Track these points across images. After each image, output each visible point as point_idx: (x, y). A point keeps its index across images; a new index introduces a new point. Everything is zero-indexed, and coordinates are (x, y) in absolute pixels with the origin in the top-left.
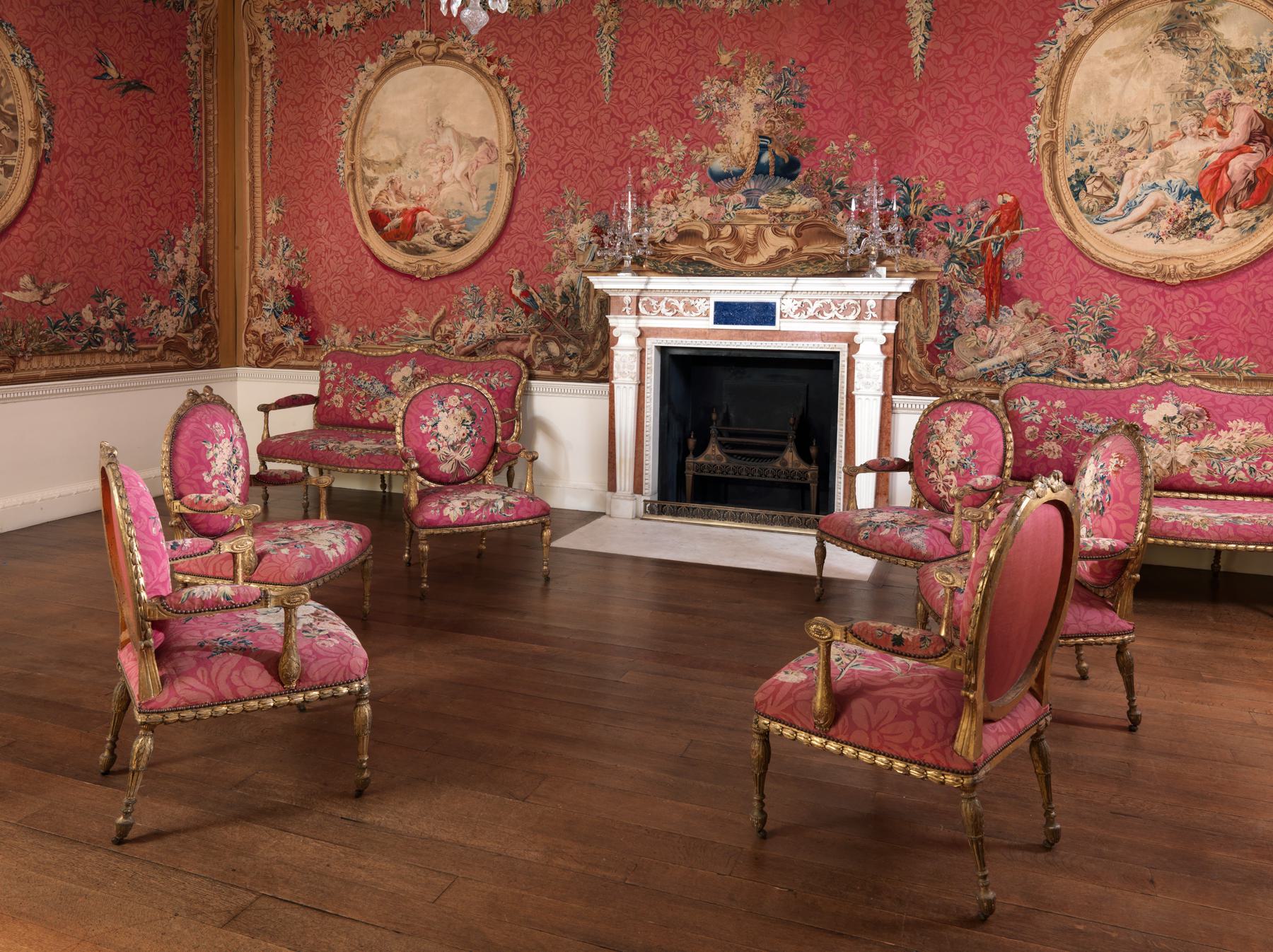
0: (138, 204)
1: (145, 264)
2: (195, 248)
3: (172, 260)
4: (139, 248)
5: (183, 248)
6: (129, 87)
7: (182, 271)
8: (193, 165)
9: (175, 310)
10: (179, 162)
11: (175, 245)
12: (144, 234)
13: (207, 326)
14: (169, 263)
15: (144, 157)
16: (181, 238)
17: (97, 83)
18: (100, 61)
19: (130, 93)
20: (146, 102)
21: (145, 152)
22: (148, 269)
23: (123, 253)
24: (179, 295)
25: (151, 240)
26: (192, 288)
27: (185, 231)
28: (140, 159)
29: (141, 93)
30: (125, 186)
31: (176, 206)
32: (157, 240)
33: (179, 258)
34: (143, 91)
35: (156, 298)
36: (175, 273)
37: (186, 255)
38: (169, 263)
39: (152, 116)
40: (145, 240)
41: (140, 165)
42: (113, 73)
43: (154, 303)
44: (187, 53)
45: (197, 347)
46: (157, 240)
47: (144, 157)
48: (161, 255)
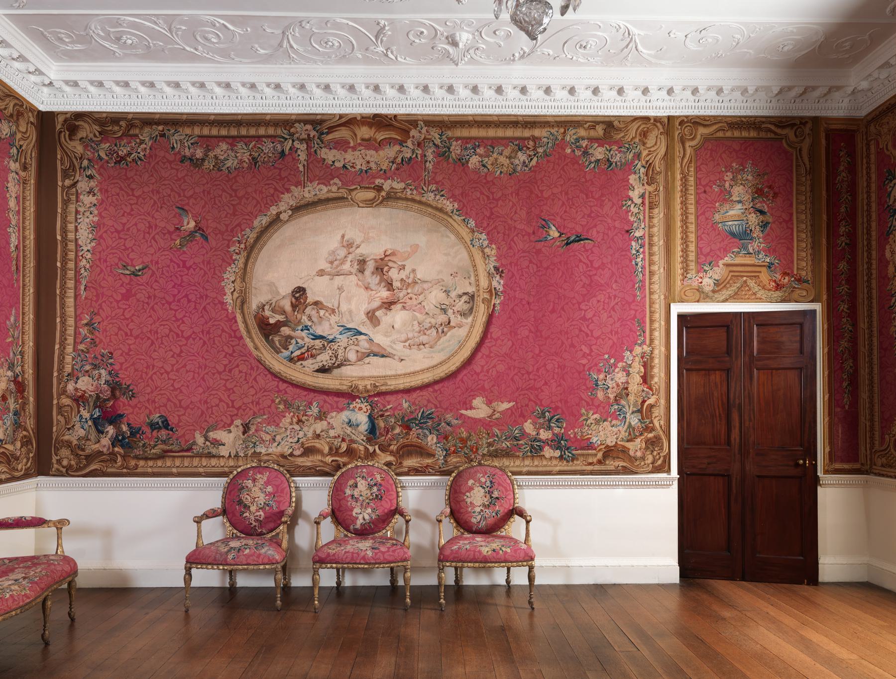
2: (637, 368)
8: (635, 296)
11: (616, 367)
13: (651, 435)
26: (635, 405)
33: (620, 377)
37: (628, 374)
44: (631, 199)
45: (639, 454)
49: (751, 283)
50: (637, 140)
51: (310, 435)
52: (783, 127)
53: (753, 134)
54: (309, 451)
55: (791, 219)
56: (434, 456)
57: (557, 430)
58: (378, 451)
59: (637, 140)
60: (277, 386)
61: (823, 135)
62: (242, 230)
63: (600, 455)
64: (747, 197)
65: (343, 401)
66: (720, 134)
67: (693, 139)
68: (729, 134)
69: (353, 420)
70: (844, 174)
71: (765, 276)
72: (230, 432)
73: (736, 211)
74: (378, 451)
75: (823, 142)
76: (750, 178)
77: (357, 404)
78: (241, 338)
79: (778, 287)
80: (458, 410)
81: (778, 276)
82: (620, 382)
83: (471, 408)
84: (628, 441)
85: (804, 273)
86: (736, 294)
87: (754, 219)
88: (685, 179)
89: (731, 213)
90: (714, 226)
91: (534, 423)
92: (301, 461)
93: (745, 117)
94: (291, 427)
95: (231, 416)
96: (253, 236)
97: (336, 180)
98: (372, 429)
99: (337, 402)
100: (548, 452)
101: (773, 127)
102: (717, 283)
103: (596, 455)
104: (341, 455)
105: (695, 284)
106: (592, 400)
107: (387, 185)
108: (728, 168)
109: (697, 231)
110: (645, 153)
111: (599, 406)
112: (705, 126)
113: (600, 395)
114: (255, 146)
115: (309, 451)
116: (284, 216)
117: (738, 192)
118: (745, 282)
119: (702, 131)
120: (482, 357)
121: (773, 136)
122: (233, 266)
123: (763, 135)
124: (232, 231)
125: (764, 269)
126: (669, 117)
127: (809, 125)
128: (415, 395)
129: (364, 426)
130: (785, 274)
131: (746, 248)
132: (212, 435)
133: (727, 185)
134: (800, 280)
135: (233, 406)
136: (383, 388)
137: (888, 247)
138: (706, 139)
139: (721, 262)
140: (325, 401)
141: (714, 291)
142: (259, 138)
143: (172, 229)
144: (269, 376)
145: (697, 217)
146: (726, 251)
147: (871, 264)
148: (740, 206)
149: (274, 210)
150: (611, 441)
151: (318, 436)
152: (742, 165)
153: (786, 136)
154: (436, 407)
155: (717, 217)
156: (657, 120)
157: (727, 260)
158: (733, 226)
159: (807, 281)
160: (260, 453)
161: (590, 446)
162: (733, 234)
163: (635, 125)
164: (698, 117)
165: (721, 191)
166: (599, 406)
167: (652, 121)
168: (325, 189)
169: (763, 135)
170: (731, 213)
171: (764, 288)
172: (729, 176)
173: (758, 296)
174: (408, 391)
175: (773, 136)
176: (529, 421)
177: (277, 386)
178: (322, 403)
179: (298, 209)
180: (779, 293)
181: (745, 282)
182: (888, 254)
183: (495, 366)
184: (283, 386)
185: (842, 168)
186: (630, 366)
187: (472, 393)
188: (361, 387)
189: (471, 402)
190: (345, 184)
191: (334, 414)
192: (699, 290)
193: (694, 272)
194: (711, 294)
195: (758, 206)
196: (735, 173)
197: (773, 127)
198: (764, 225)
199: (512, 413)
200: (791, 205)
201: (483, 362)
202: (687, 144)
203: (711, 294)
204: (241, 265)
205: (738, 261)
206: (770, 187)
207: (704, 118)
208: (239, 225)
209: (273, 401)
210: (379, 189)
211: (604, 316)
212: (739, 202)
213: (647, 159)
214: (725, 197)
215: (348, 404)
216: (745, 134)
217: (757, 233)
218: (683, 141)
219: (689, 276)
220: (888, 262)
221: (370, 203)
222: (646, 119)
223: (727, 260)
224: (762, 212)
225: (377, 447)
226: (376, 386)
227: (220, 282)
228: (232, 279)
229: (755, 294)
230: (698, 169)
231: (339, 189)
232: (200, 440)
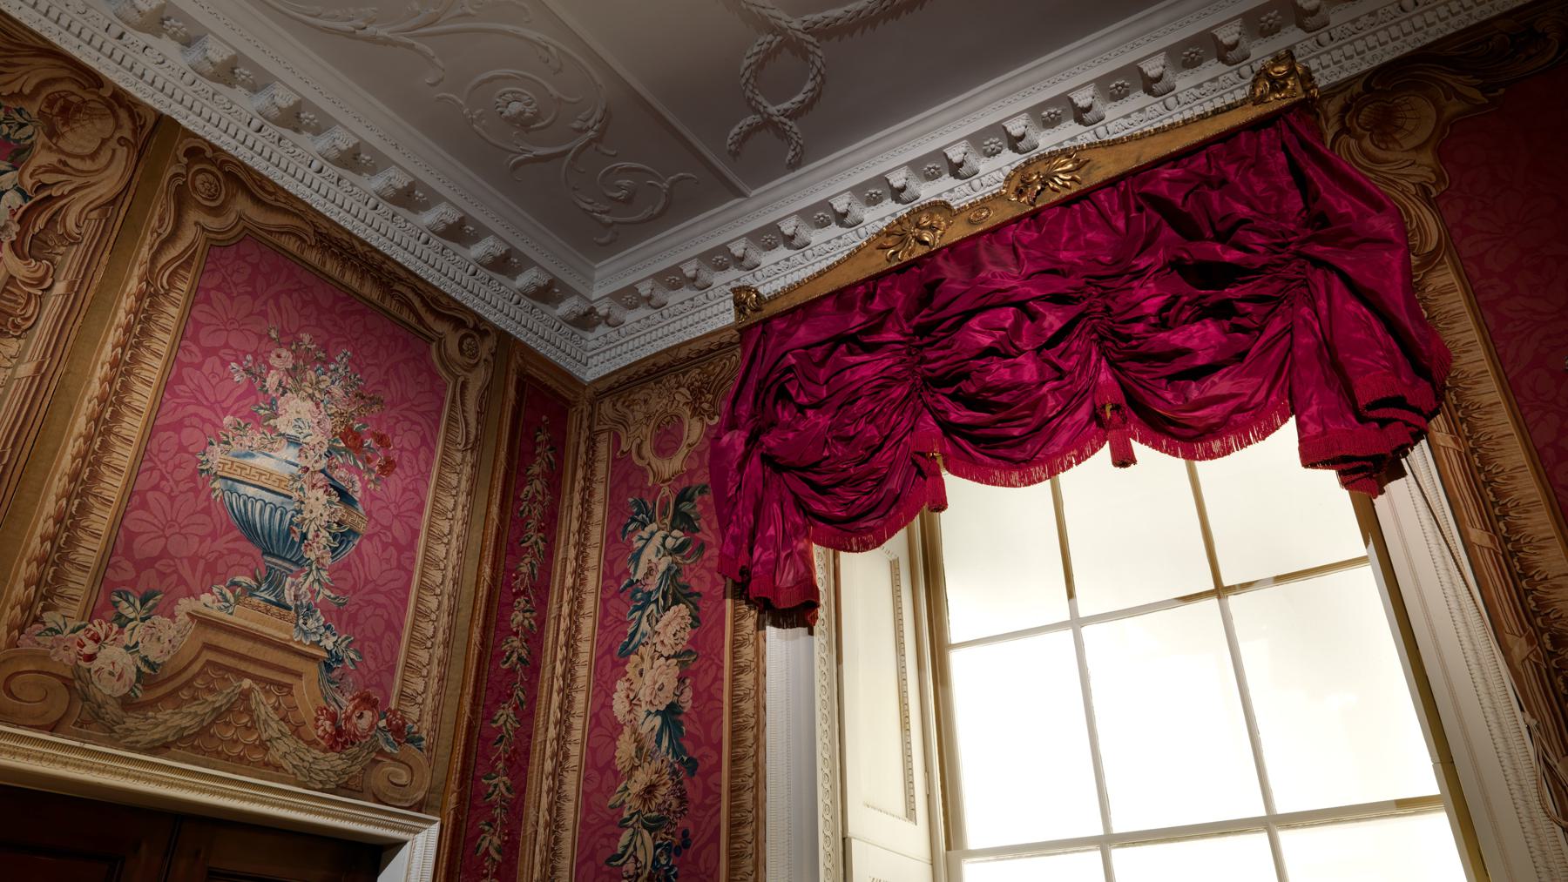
49: (264, 704)
50: (33, 109)
52: (440, 316)
53: (370, 291)
55: (411, 546)
59: (33, 109)
61: (513, 378)
64: (317, 438)
66: (291, 245)
67: (215, 212)
68: (313, 257)
70: (538, 485)
71: (308, 693)
73: (277, 462)
75: (512, 392)
76: (337, 391)
79: (340, 738)
81: (347, 704)
85: (413, 712)
86: (204, 731)
87: (318, 506)
88: (149, 302)
89: (261, 461)
90: (199, 477)
93: (363, 243)
101: (417, 303)
102: (150, 675)
105: (65, 658)
108: (288, 338)
109: (137, 471)
110: (43, 158)
112: (258, 201)
117: (297, 413)
118: (245, 695)
119: (242, 205)
121: (413, 321)
123: (391, 305)
125: (312, 670)
126: (161, 119)
127: (490, 343)
130: (366, 701)
131: (275, 584)
133: (272, 380)
134: (400, 732)
137: (621, 685)
138: (249, 234)
139: (185, 605)
141: (127, 703)
145: (152, 431)
146: (213, 573)
147: (569, 728)
148: (291, 453)
152: (325, 347)
153: (441, 341)
155: (216, 457)
156: (120, 101)
157: (208, 603)
158: (257, 502)
159: (415, 740)
162: (248, 529)
163: (43, 70)
164: (248, 170)
165: (250, 391)
167: (106, 93)
169: (391, 305)
170: (261, 461)
171: (297, 731)
172: (282, 359)
173: (274, 756)
175: (413, 321)
180: (335, 761)
181: (245, 695)
182: (620, 706)
185: (536, 469)
192: (75, 684)
193: (75, 609)
194: (113, 710)
195: (340, 474)
196: (304, 361)
197: (417, 303)
198: (343, 536)
200: (420, 509)
202: (193, 216)
203: (113, 710)
205: (241, 617)
206: (381, 439)
207: (262, 181)
212: (293, 442)
213: (48, 178)
214: (257, 410)
216: (351, 279)
217: (318, 550)
218: (182, 200)
219: (51, 618)
220: (618, 728)
222: (94, 79)
223: (208, 603)
224: (344, 496)
229: (264, 746)
230: (199, 296)
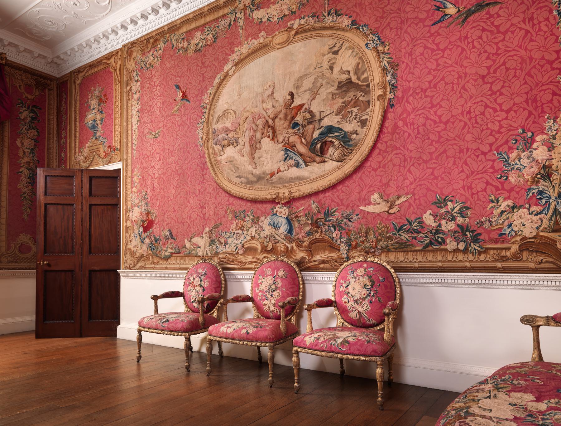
0: (483, 114)
1: (492, 167)
3: (528, 158)
4: (484, 154)
5: (544, 143)
6: (469, 13)
7: (545, 167)
9: (534, 208)
10: (537, 55)
11: (533, 140)
12: (491, 139)
14: (525, 162)
15: (488, 68)
16: (543, 133)
17: (434, 29)
18: (438, 8)
19: (471, 18)
20: (491, 16)
21: (489, 63)
22: (496, 171)
23: (466, 163)
24: (541, 193)
25: (499, 143)
27: (549, 124)
28: (484, 72)
29: (483, 13)
30: (466, 102)
31: (535, 101)
32: (507, 142)
34: (486, 9)
35: (508, 198)
36: (535, 169)
38: (525, 162)
39: (498, 27)
40: (491, 145)
41: (483, 77)
42: (451, 10)
43: (504, 205)
46: (507, 142)
47: (488, 68)
48: (514, 155)
51: (249, 238)
54: (249, 250)
56: (339, 250)
57: (460, 220)
58: (295, 247)
60: (228, 200)
62: (207, 90)
63: (515, 248)
65: (269, 206)
69: (276, 222)
72: (202, 237)
74: (295, 247)
77: (278, 208)
78: (208, 168)
80: (358, 206)
82: (539, 158)
83: (370, 203)
84: (554, 231)
91: (435, 215)
92: (243, 258)
94: (237, 232)
95: (203, 226)
96: (214, 91)
97: (263, 33)
98: (290, 231)
99: (265, 208)
100: (451, 245)
103: (509, 249)
104: (268, 252)
106: (502, 184)
107: (296, 23)
111: (510, 191)
113: (513, 178)
114: (215, 27)
115: (249, 250)
116: (230, 73)
120: (379, 154)
122: (203, 117)
124: (202, 91)
128: (321, 196)
129: (284, 228)
132: (195, 240)
135: (204, 218)
136: (297, 194)
140: (258, 209)
142: (216, 20)
143: (172, 101)
144: (224, 193)
149: (226, 69)
150: (529, 232)
151: (253, 238)
154: (338, 205)
160: (220, 252)
161: (501, 237)
166: (510, 191)
168: (255, 42)
174: (316, 193)
176: (429, 212)
177: (228, 200)
178: (255, 210)
179: (239, 64)
183: (391, 160)
184: (231, 199)
186: (554, 137)
187: (371, 189)
188: (281, 195)
189: (369, 197)
190: (268, 34)
191: (264, 217)
199: (410, 205)
201: (381, 158)
204: (206, 116)
208: (206, 87)
209: (226, 212)
210: (291, 28)
211: (517, 84)
215: (273, 209)
221: (288, 42)
225: (294, 245)
226: (291, 193)
227: (195, 131)
228: (202, 127)
231: (265, 39)
232: (188, 245)
